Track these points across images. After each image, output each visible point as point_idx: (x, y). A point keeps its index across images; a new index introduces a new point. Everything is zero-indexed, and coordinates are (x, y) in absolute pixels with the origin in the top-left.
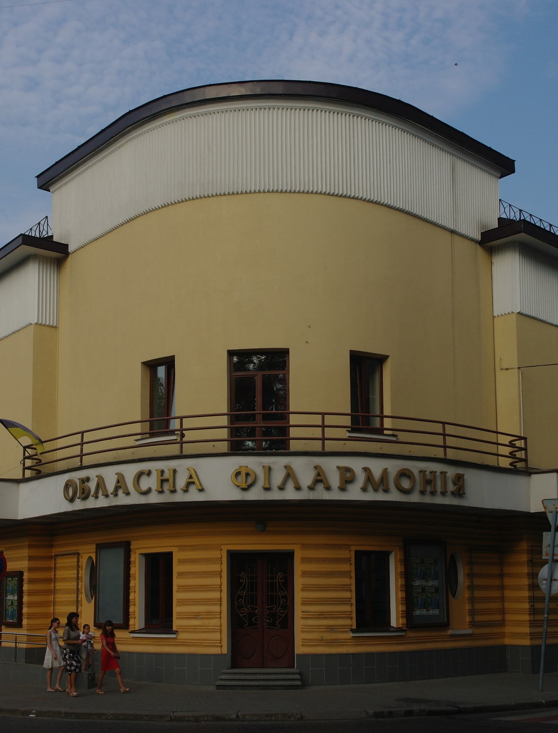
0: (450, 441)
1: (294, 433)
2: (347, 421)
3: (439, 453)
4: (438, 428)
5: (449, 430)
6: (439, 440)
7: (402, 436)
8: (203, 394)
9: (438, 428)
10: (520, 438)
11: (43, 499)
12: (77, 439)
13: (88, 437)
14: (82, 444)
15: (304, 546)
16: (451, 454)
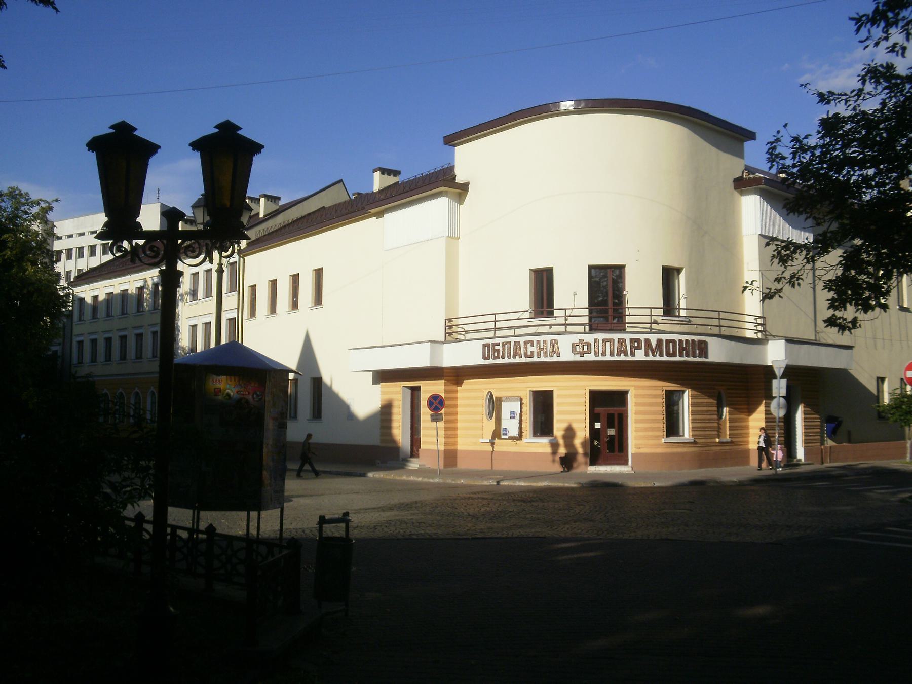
0: (723, 323)
1: (628, 319)
2: (661, 312)
3: (716, 330)
4: (716, 315)
5: (722, 315)
6: (716, 322)
7: (695, 321)
8: (572, 294)
9: (716, 315)
10: (760, 317)
11: (468, 354)
12: (492, 318)
13: (499, 317)
14: (495, 321)
15: (637, 387)
16: (724, 331)
